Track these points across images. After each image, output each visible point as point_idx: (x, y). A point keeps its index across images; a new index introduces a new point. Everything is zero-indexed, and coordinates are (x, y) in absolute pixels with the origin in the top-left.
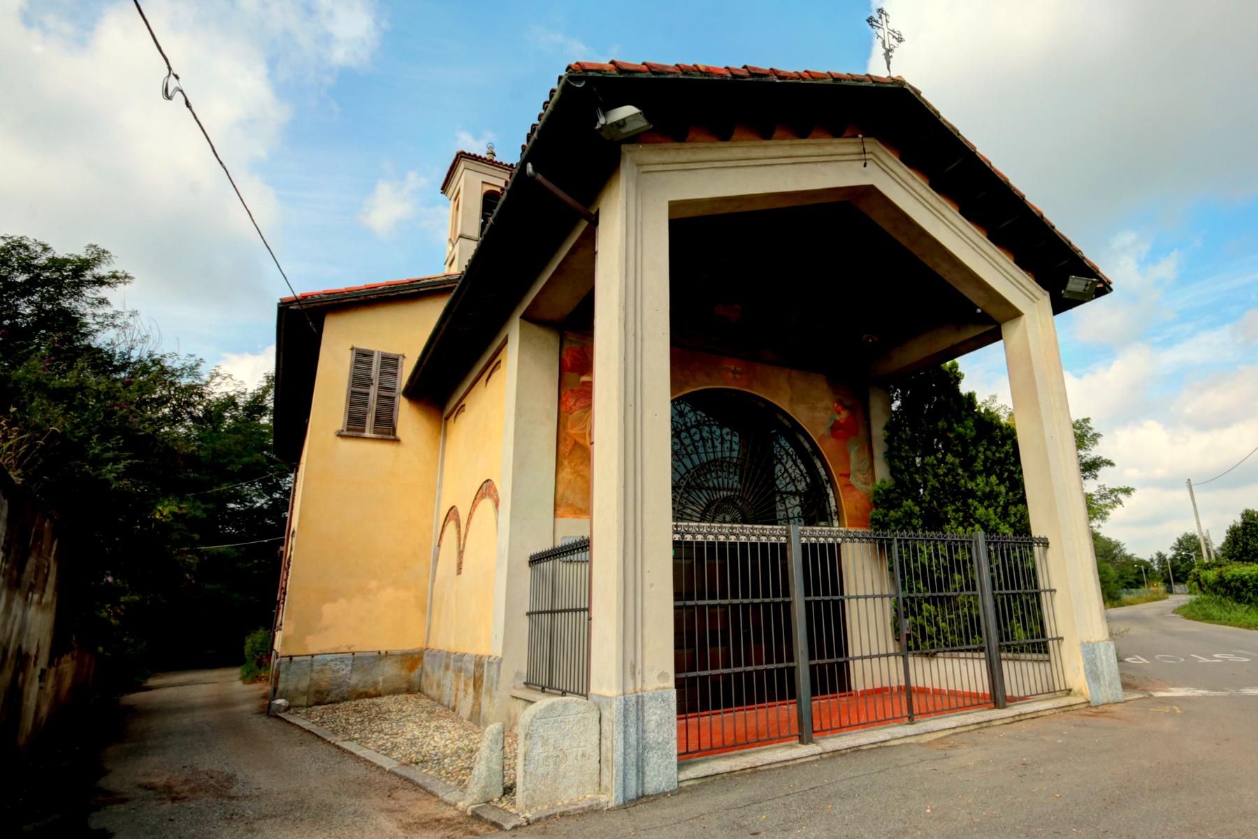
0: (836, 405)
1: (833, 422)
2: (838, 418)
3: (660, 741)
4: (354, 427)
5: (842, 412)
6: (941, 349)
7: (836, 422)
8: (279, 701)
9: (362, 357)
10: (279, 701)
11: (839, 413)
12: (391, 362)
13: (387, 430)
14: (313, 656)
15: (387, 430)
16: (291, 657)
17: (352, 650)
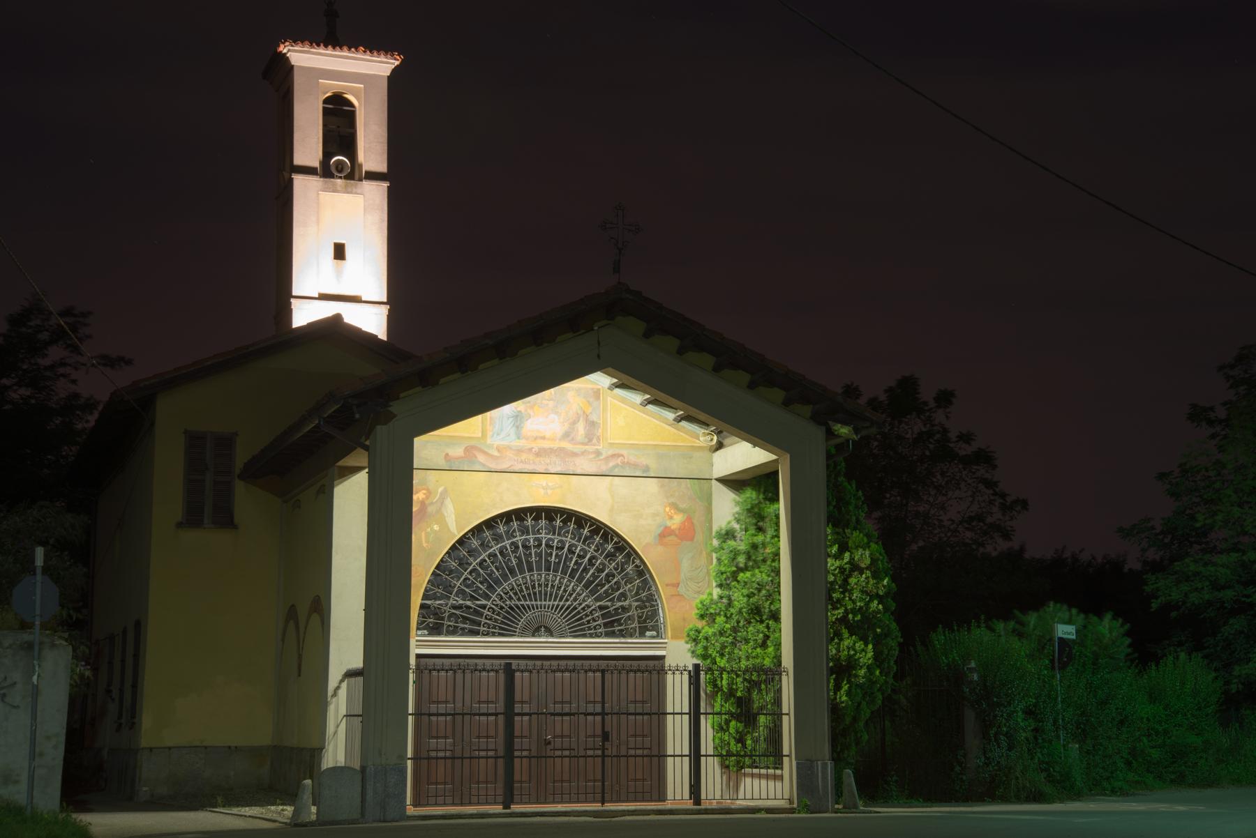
0: (668, 509)
1: (662, 528)
2: (669, 523)
3: (396, 792)
4: (192, 518)
5: (675, 517)
6: (779, 450)
7: (666, 528)
8: (145, 789)
9: (195, 441)
10: (145, 789)
11: (671, 518)
12: (226, 443)
13: (225, 519)
14: (170, 748)
15: (225, 519)
16: (151, 749)
17: (204, 744)
